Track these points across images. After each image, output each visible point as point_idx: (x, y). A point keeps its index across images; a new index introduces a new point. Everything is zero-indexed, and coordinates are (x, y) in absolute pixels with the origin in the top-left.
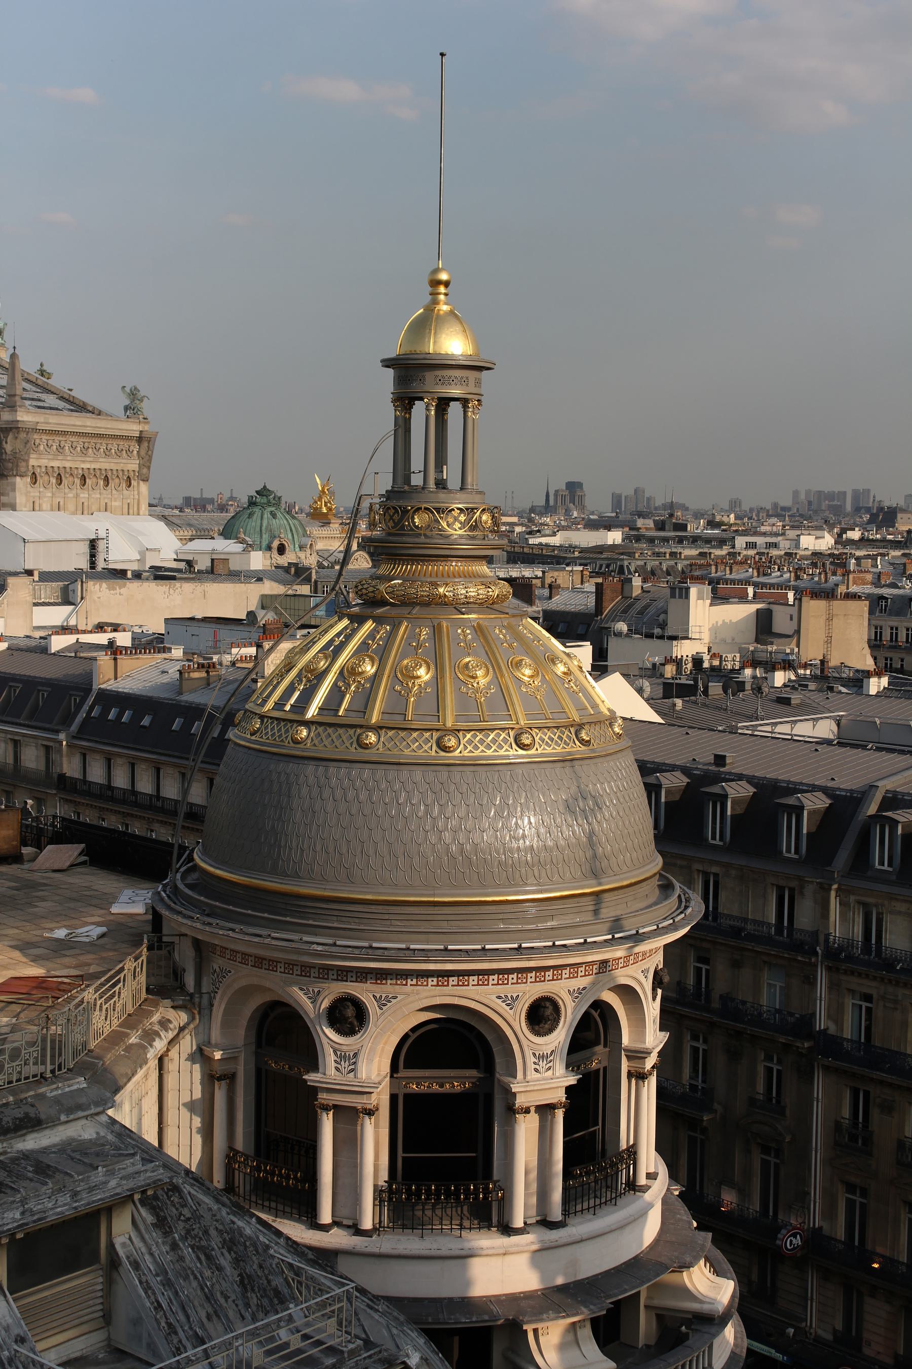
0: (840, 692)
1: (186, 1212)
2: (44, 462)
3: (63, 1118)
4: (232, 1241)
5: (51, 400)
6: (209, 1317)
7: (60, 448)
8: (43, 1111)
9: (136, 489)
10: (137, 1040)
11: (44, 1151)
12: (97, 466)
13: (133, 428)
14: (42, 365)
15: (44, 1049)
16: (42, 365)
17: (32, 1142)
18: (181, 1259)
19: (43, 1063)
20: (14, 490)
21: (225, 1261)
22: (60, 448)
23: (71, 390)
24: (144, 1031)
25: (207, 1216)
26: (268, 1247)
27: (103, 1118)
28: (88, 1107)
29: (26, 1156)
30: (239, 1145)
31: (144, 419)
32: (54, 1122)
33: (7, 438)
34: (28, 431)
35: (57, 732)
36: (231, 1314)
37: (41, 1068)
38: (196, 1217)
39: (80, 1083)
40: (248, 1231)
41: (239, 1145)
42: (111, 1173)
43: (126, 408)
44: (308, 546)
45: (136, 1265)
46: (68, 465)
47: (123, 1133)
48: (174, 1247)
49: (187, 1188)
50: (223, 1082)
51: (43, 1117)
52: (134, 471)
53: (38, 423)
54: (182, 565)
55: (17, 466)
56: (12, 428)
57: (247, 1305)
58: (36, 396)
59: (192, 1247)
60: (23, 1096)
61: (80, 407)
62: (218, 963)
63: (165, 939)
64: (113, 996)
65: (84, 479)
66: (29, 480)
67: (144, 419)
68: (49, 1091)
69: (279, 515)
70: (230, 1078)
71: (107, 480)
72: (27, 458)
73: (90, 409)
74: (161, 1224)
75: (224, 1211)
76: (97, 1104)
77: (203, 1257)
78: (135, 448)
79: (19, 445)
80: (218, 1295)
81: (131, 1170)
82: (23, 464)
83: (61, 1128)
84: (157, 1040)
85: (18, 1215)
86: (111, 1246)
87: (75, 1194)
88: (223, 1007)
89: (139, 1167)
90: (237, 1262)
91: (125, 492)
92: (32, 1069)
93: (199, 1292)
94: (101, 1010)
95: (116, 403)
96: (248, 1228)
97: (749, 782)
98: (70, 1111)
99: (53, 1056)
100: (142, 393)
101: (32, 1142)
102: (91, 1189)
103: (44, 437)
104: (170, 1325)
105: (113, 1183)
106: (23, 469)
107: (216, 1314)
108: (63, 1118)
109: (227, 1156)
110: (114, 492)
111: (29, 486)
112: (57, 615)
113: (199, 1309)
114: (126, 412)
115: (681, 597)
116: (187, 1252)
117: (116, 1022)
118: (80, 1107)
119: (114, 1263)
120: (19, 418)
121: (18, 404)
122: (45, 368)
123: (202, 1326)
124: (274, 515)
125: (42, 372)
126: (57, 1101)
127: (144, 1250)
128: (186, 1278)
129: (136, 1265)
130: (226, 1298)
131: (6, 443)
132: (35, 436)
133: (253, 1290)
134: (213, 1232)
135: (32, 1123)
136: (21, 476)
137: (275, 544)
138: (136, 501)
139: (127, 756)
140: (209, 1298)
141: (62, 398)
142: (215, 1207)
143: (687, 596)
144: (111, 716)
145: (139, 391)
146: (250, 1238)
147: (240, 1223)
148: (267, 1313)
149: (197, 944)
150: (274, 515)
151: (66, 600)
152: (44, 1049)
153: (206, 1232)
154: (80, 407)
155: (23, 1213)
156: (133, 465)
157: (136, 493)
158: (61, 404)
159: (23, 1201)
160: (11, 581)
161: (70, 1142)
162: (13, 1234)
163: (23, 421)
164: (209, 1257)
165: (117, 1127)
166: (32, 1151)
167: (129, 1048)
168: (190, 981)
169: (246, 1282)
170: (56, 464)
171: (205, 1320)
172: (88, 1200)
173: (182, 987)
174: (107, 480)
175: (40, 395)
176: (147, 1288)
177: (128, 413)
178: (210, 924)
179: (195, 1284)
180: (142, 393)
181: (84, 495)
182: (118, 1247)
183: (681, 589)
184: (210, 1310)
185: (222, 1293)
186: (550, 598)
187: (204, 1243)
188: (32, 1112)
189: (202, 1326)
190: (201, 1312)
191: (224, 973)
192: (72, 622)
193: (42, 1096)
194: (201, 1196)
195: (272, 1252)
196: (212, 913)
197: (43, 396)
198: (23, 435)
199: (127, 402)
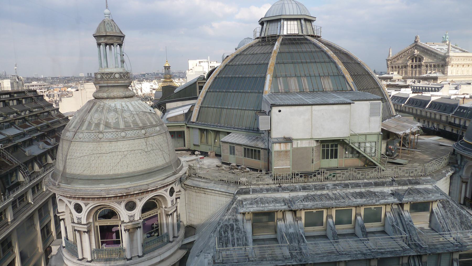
1: (450, 206)
2: (455, 63)
3: (425, 184)
4: (460, 214)
5: (457, 50)
6: (452, 227)
7: (458, 60)
8: (421, 181)
10: (444, 172)
11: (420, 189)
15: (422, 170)
17: (418, 187)
18: (448, 215)
19: (422, 173)
21: (458, 217)
22: (458, 60)
24: (446, 170)
25: (455, 208)
26: (468, 217)
27: (434, 185)
28: (430, 182)
29: (416, 189)
30: (467, 196)
32: (423, 184)
34: (451, 57)
35: (450, 114)
36: (457, 228)
37: (421, 174)
38: (452, 207)
39: (429, 178)
40: (464, 213)
41: (467, 196)
42: (433, 195)
45: (437, 214)
46: (460, 63)
47: (438, 189)
48: (446, 212)
49: (451, 202)
50: (465, 183)
51: (420, 182)
56: (449, 56)
57: (461, 227)
59: (450, 213)
60: (417, 178)
62: (465, 160)
63: (455, 154)
64: (440, 162)
65: (463, 65)
68: (423, 178)
70: (467, 183)
74: (444, 207)
75: (459, 208)
76: (432, 182)
77: (452, 216)
79: (449, 60)
80: (455, 224)
81: (438, 196)
83: (424, 185)
84: (449, 172)
85: (412, 199)
86: (432, 209)
87: (424, 198)
88: (466, 169)
89: (440, 196)
90: (460, 218)
92: (420, 174)
93: (450, 222)
94: (436, 165)
96: (464, 212)
98: (427, 182)
99: (424, 172)
101: (418, 187)
102: (428, 198)
103: (455, 58)
104: (443, 226)
105: (433, 197)
107: (454, 227)
108: (425, 184)
109: (464, 198)
112: (455, 92)
113: (450, 225)
116: (449, 214)
117: (440, 168)
118: (428, 182)
119: (432, 212)
123: (450, 228)
126: (424, 180)
127: (439, 211)
128: (448, 219)
129: (437, 214)
130: (457, 224)
132: (453, 58)
133: (463, 224)
134: (455, 211)
135: (418, 183)
139: (459, 118)
140: (453, 223)
141: (460, 50)
142: (457, 207)
144: (462, 111)
146: (464, 214)
147: (462, 211)
148: (466, 230)
149: (461, 156)
151: (456, 88)
152: (422, 170)
153: (454, 211)
155: (413, 199)
158: (460, 51)
159: (413, 197)
160: (445, 85)
161: (426, 188)
162: (411, 202)
164: (454, 216)
165: (436, 187)
166: (418, 188)
167: (442, 173)
168: (459, 162)
169: (462, 223)
170: (457, 63)
171: (451, 227)
172: (426, 200)
173: (457, 163)
176: (439, 218)
178: (464, 152)
179: (450, 220)
181: (463, 68)
182: (433, 209)
184: (453, 226)
185: (456, 223)
187: (453, 213)
188: (418, 181)
189: (450, 228)
190: (450, 226)
191: (466, 162)
192: (457, 93)
193: (421, 179)
194: (454, 204)
195: (469, 218)
196: (465, 149)
198: (450, 58)
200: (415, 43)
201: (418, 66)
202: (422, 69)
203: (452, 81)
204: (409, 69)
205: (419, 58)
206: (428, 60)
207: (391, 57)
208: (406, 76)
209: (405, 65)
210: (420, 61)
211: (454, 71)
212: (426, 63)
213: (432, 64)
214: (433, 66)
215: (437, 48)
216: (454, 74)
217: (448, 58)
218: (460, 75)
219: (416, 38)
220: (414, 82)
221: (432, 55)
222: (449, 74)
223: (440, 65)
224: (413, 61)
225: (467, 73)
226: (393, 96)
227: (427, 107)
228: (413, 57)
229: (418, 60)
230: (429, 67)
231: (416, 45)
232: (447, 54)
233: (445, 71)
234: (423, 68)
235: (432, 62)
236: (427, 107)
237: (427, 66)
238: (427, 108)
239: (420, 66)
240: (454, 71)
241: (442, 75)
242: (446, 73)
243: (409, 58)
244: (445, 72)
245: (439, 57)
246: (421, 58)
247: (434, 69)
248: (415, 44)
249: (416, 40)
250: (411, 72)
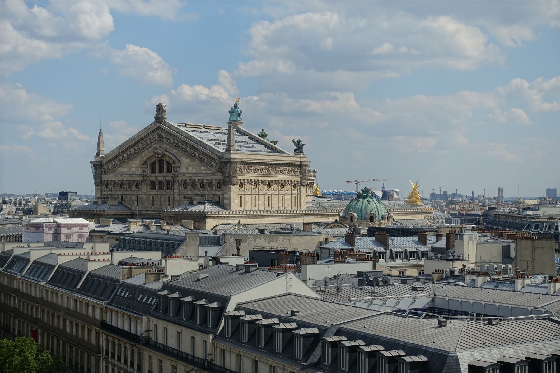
0: (458, 285)
2: (246, 178)
5: (260, 147)
9: (299, 190)
12: (277, 179)
13: (297, 160)
14: (263, 130)
16: (263, 130)
20: (230, 191)
23: (275, 143)
31: (304, 155)
33: (226, 166)
34: (236, 163)
43: (295, 150)
44: (387, 217)
46: (260, 178)
52: (298, 181)
53: (242, 159)
54: (289, 227)
55: (231, 179)
58: (252, 145)
61: (275, 150)
66: (238, 186)
67: (304, 155)
69: (371, 201)
71: (283, 185)
72: (236, 175)
73: (279, 151)
78: (298, 170)
82: (235, 179)
91: (293, 192)
95: (290, 149)
97: (297, 323)
100: (302, 143)
106: (234, 182)
110: (286, 192)
111: (238, 189)
114: (295, 152)
115: (460, 239)
120: (232, 157)
121: (232, 150)
122: (264, 131)
124: (369, 202)
125: (263, 135)
131: (226, 168)
136: (234, 185)
137: (368, 217)
138: (299, 196)
143: (462, 239)
145: (301, 142)
150: (369, 202)
154: (275, 150)
156: (297, 178)
157: (299, 192)
163: (234, 158)
170: (253, 178)
174: (283, 185)
175: (252, 145)
177: (296, 153)
180: (302, 143)
183: (460, 235)
186: (437, 241)
197: (256, 145)
199: (296, 147)
200: (156, 122)
201: (165, 183)
202: (175, 191)
203: (239, 224)
204: (145, 189)
205: (168, 163)
206: (187, 169)
207: (103, 158)
208: (140, 209)
209: (136, 179)
210: (169, 171)
211: (248, 198)
212: (184, 174)
213: (197, 179)
214: (199, 185)
215: (208, 140)
216: (248, 208)
217: (228, 165)
218: (262, 208)
219: (160, 108)
220: (147, 227)
221: (195, 156)
222: (235, 206)
223: (215, 182)
224: (153, 171)
225: (280, 205)
226: (34, 262)
227: (78, 287)
228: (153, 160)
229: (165, 166)
230: (189, 187)
231: (159, 128)
232: (227, 156)
233: (226, 199)
234: (177, 189)
235: (196, 175)
236: (78, 287)
237: (185, 185)
238: (79, 289)
239: (170, 185)
240: (248, 198)
241: (216, 209)
242: (226, 204)
243: (145, 163)
244: (226, 201)
245: (209, 161)
246: (172, 163)
247: (202, 192)
248: (158, 124)
249: (160, 116)
250: (151, 198)
